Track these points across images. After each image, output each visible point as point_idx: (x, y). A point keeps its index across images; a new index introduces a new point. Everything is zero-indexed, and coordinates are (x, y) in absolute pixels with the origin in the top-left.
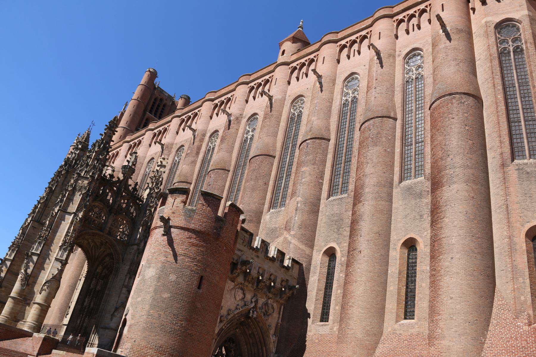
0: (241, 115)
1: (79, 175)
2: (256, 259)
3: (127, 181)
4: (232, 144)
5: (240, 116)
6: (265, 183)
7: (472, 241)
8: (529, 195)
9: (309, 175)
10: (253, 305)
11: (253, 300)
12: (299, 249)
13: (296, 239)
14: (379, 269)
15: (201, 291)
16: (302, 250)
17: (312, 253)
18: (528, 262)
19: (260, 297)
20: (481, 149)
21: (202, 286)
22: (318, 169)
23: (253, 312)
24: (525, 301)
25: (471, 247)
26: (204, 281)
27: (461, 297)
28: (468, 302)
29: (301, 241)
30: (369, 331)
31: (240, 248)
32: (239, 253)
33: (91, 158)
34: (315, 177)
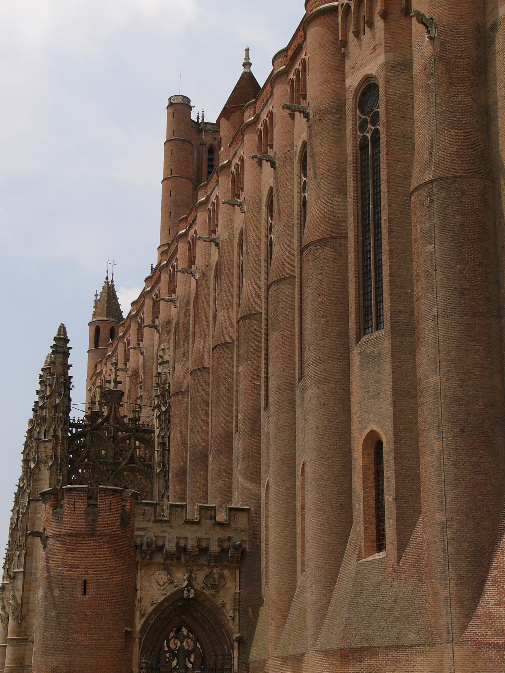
0: (207, 266)
1: (38, 439)
2: (170, 530)
3: (116, 412)
4: (206, 320)
5: (207, 268)
6: (228, 389)
7: (322, 464)
8: (367, 389)
9: (244, 378)
10: (186, 582)
11: (185, 578)
12: (246, 489)
13: (242, 476)
14: (286, 507)
15: (87, 596)
16: (249, 489)
17: (259, 490)
18: (364, 482)
19: (198, 570)
20: (339, 325)
21: (87, 591)
22: (252, 366)
23: (189, 591)
24: (360, 532)
25: (321, 472)
26: (88, 586)
27: (313, 538)
28: (318, 543)
29: (245, 478)
30: (281, 588)
31: (141, 526)
32: (142, 533)
33: (46, 408)
34: (250, 378)
